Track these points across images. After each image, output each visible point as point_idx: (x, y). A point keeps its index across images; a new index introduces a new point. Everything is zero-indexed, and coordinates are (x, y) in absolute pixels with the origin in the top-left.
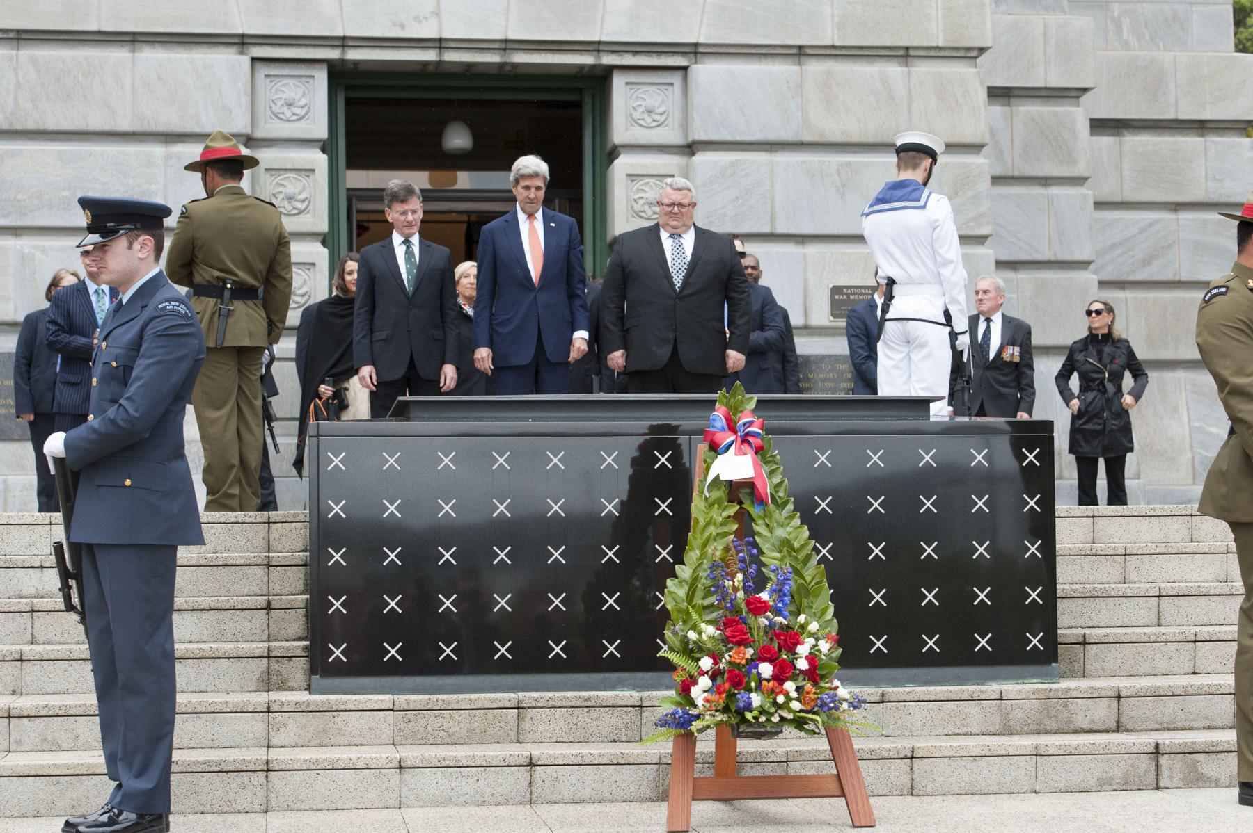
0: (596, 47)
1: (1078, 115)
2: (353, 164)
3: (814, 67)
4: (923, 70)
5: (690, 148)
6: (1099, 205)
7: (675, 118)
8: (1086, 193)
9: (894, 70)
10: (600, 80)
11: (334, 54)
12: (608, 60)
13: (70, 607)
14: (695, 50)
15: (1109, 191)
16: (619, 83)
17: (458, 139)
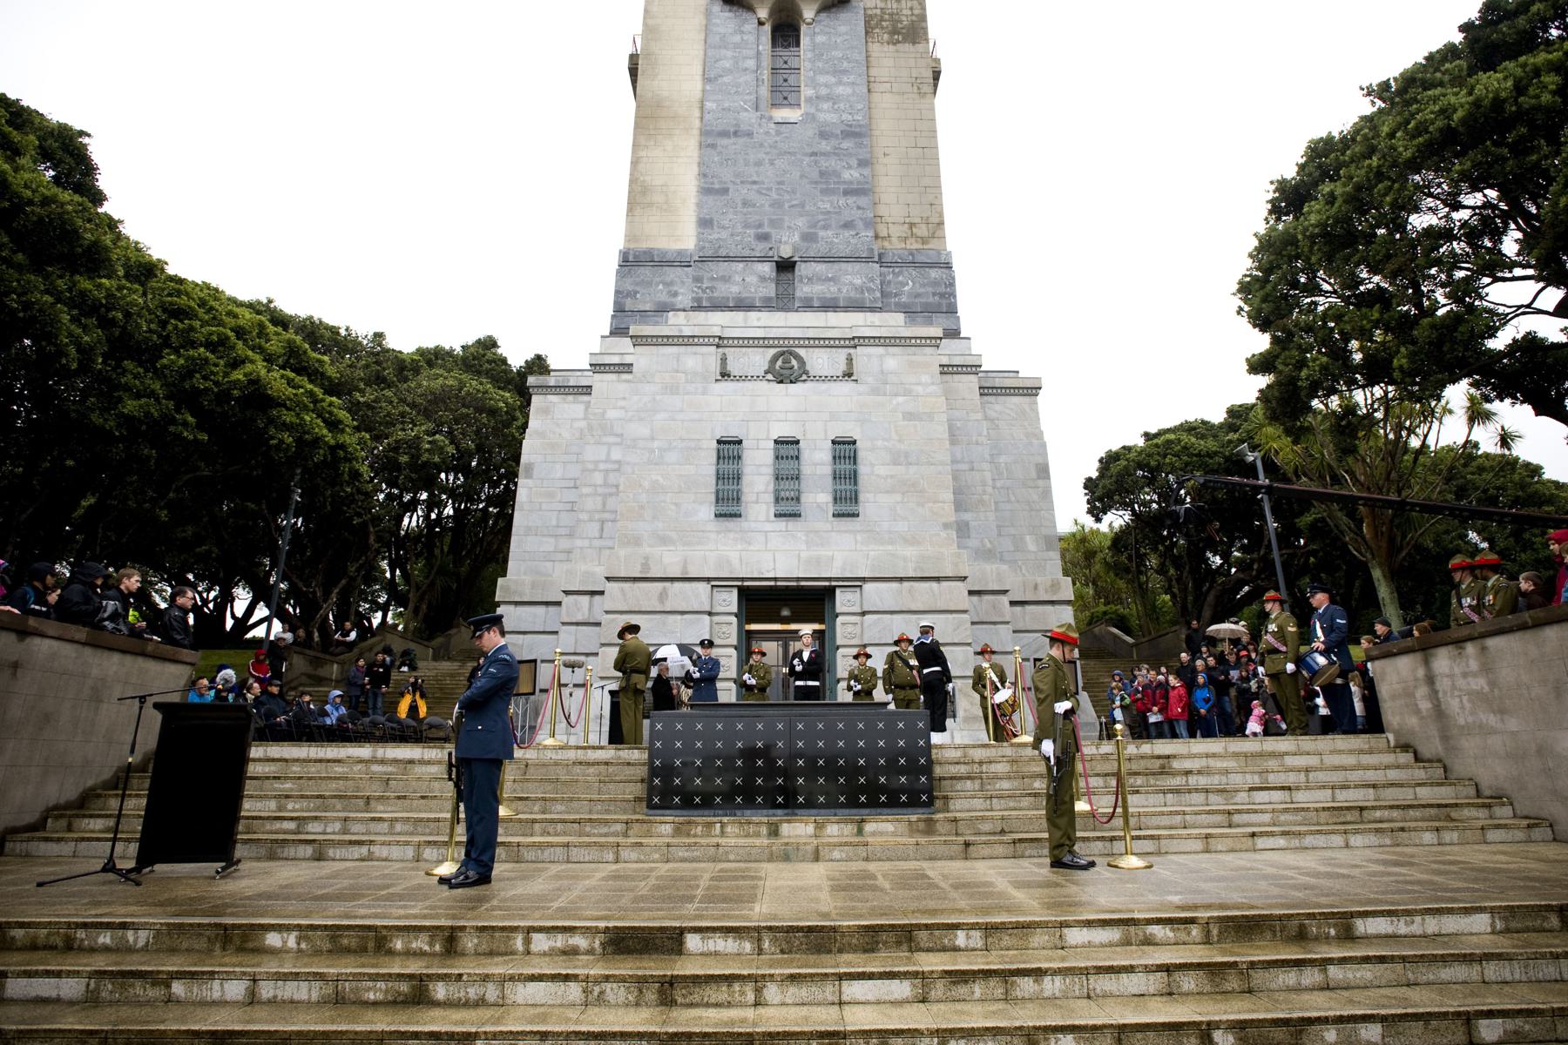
0: (829, 579)
1: (1005, 600)
2: (749, 622)
3: (906, 584)
4: (945, 584)
5: (863, 614)
6: (1014, 632)
7: (858, 603)
8: (1009, 627)
9: (934, 585)
10: (831, 591)
11: (739, 583)
12: (834, 583)
13: (450, 779)
14: (864, 580)
15: (1021, 626)
16: (838, 591)
17: (785, 613)
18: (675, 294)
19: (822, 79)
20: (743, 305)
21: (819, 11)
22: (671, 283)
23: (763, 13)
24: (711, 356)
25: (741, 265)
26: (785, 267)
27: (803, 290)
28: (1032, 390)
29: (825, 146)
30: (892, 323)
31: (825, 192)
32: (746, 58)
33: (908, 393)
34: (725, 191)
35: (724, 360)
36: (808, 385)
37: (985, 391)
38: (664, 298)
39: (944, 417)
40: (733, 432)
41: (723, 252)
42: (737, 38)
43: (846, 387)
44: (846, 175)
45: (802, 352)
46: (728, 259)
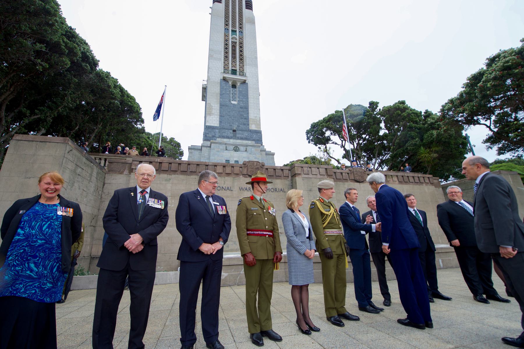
18: (216, 134)
19: (241, 97)
20: (228, 137)
21: (241, 84)
22: (215, 132)
23: (230, 83)
24: (224, 146)
25: (227, 130)
26: (234, 131)
27: (238, 136)
28: (273, 154)
29: (241, 110)
30: (253, 143)
31: (242, 118)
32: (227, 91)
33: (255, 154)
34: (224, 116)
35: (226, 147)
36: (240, 152)
37: (266, 154)
38: (214, 135)
39: (261, 159)
40: (228, 159)
41: (224, 128)
42: (225, 87)
43: (246, 153)
44: (245, 116)
45: (239, 147)
46: (224, 129)
